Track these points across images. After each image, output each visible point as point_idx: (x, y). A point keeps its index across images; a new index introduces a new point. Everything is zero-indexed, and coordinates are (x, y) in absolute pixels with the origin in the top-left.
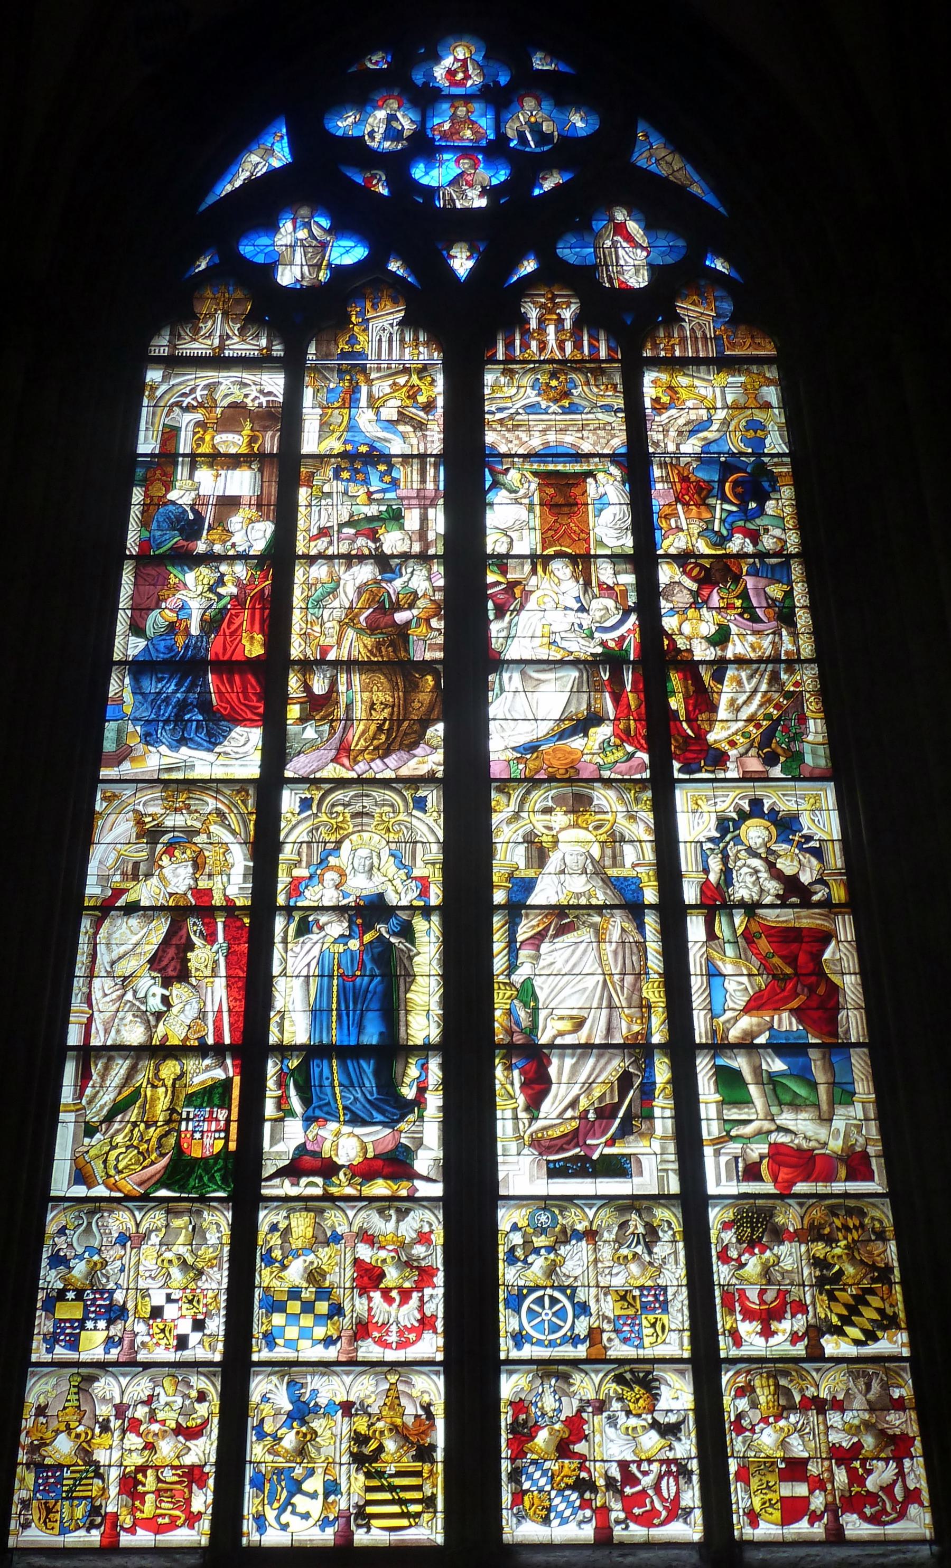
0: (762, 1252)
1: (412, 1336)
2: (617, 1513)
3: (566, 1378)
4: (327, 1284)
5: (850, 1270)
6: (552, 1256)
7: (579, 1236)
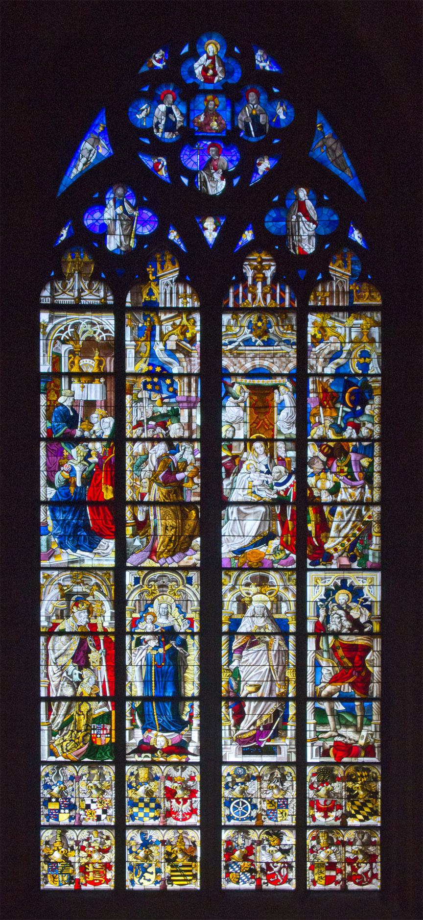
2: (264, 880)
3: (247, 833)
5: (361, 793)
7: (254, 778)
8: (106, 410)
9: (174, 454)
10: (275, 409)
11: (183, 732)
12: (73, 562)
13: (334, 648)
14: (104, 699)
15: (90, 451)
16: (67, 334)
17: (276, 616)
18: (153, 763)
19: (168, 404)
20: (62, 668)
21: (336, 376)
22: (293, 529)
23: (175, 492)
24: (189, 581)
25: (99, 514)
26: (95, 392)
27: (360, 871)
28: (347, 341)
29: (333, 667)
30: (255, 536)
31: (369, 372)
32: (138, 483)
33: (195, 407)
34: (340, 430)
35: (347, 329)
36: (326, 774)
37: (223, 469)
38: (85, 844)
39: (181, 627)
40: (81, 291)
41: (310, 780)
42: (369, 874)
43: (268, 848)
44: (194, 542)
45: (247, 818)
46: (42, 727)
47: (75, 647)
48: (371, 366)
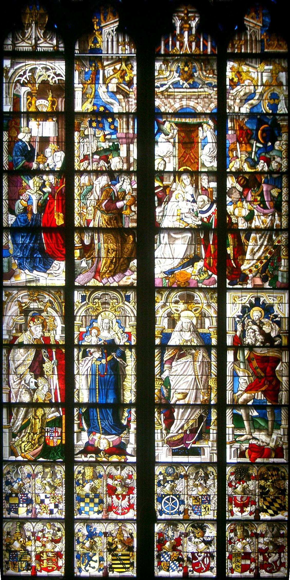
0: (243, 483)
1: (126, 511)
2: (190, 568)
4: (98, 492)
5: (272, 490)
6: (173, 484)
7: (182, 477)
8: (58, 145)
10: (200, 144)
11: (122, 435)
12: (30, 282)
13: (249, 360)
14: (56, 405)
15: (45, 181)
16: (26, 78)
17: (201, 331)
18: (98, 463)
19: (109, 140)
20: (21, 377)
21: (251, 115)
22: (214, 252)
23: (116, 219)
24: (128, 298)
25: (51, 237)
26: (49, 129)
27: (270, 560)
28: (259, 84)
29: (248, 376)
30: (183, 259)
31: (278, 112)
32: (85, 210)
33: (132, 143)
34: (254, 164)
35: (260, 74)
36: (242, 472)
37: (156, 198)
38: (40, 534)
39: (121, 341)
40: (37, 39)
41: (229, 479)
42: (278, 563)
43: (193, 539)
44: (131, 264)
45: (176, 513)
46: (4, 430)
47: (31, 358)
48: (279, 106)
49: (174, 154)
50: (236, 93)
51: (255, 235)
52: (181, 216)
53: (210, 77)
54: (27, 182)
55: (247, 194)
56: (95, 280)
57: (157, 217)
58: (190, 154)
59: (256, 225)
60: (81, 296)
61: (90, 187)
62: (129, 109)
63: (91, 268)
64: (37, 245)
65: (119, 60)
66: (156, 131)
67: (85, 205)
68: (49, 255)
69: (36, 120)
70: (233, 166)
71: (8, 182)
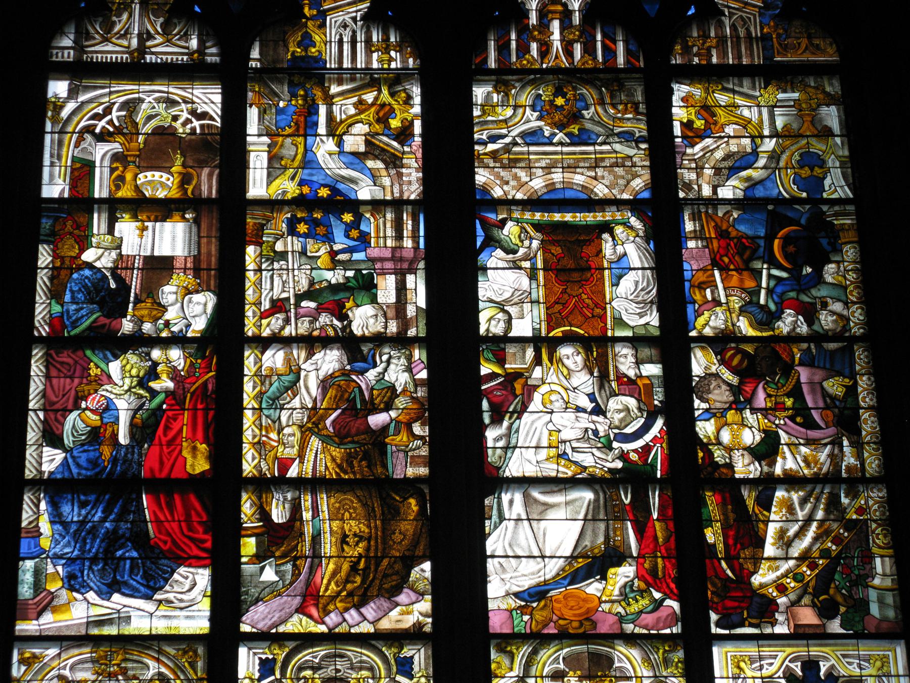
8: (196, 276)
9: (362, 372)
10: (606, 272)
15: (155, 364)
19: (346, 265)
21: (747, 203)
22: (667, 540)
23: (366, 456)
24: (405, 667)
25: (171, 507)
28: (766, 132)
30: (572, 558)
32: (274, 436)
33: (413, 271)
35: (765, 111)
37: (485, 405)
44: (415, 573)
49: (534, 296)
50: (701, 154)
51: (785, 494)
52: (562, 447)
53: (629, 119)
54: (103, 365)
55: (754, 392)
56: (304, 618)
57: (490, 452)
58: (579, 296)
59: (787, 467)
60: (257, 662)
61: (291, 378)
62: (401, 192)
63: (291, 584)
64: (124, 526)
65: (371, 79)
66: (479, 244)
67: (274, 422)
68: (162, 551)
69: (135, 217)
70: (710, 323)
71: (47, 367)
